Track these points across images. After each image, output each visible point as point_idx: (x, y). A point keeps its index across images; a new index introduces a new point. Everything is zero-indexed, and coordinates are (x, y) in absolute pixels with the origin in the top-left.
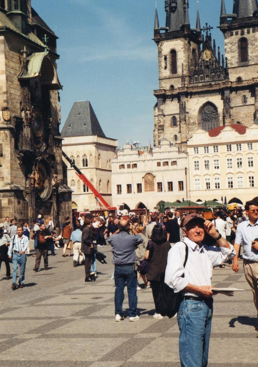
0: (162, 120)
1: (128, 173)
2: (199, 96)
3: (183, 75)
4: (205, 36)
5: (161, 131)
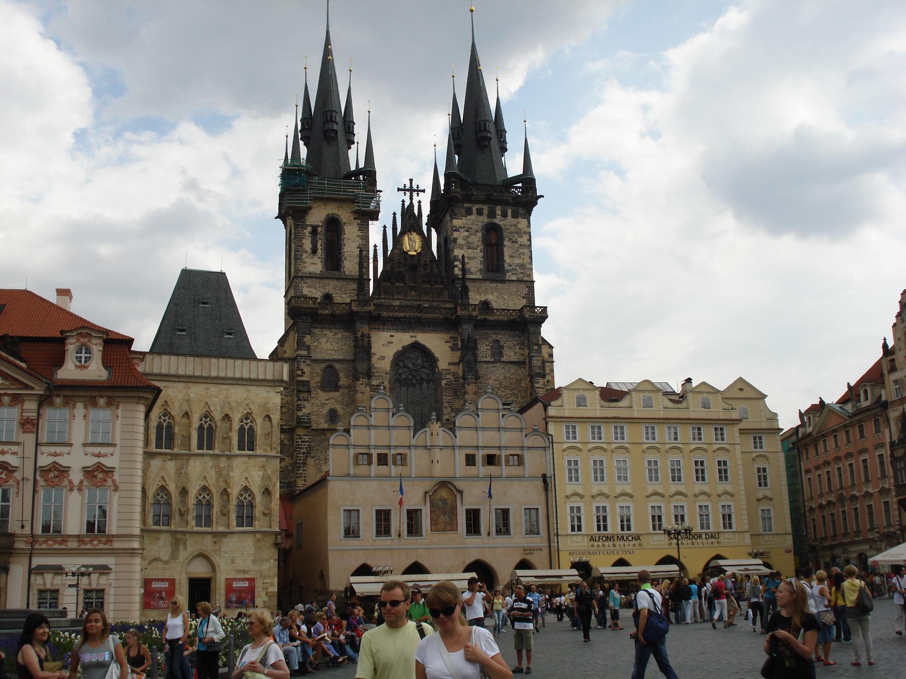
0: (306, 369)
1: (379, 477)
4: (407, 204)
5: (306, 394)
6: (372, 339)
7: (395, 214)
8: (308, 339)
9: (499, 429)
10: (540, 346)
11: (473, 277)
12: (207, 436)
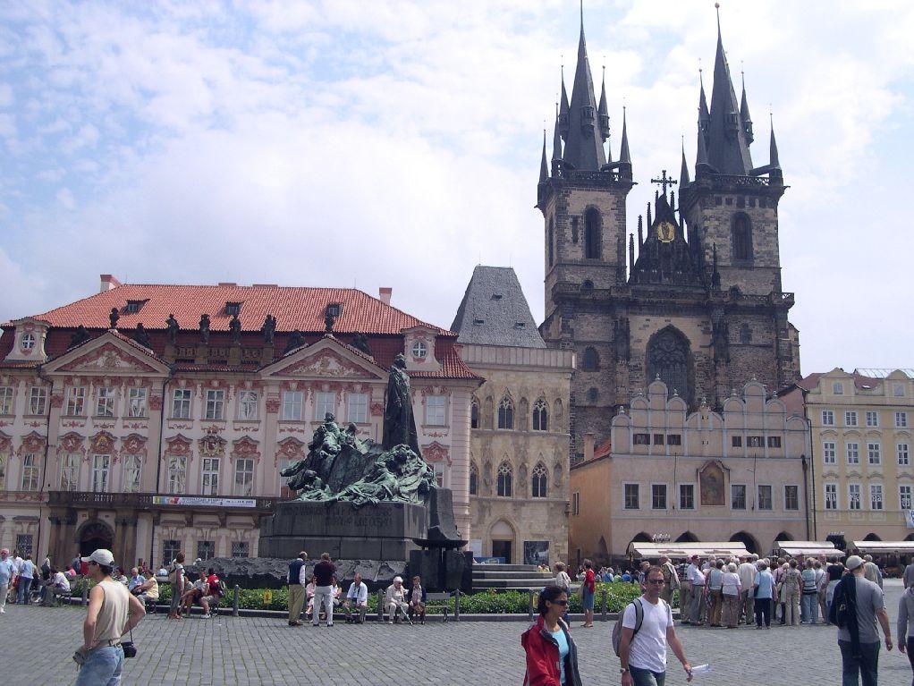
2: (651, 312)
3: (619, 262)
6: (631, 325)
7: (649, 204)
8: (571, 322)
9: (763, 414)
10: (786, 331)
11: (724, 264)
12: (506, 418)
